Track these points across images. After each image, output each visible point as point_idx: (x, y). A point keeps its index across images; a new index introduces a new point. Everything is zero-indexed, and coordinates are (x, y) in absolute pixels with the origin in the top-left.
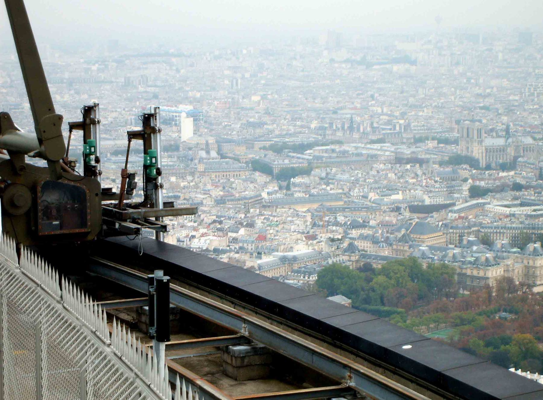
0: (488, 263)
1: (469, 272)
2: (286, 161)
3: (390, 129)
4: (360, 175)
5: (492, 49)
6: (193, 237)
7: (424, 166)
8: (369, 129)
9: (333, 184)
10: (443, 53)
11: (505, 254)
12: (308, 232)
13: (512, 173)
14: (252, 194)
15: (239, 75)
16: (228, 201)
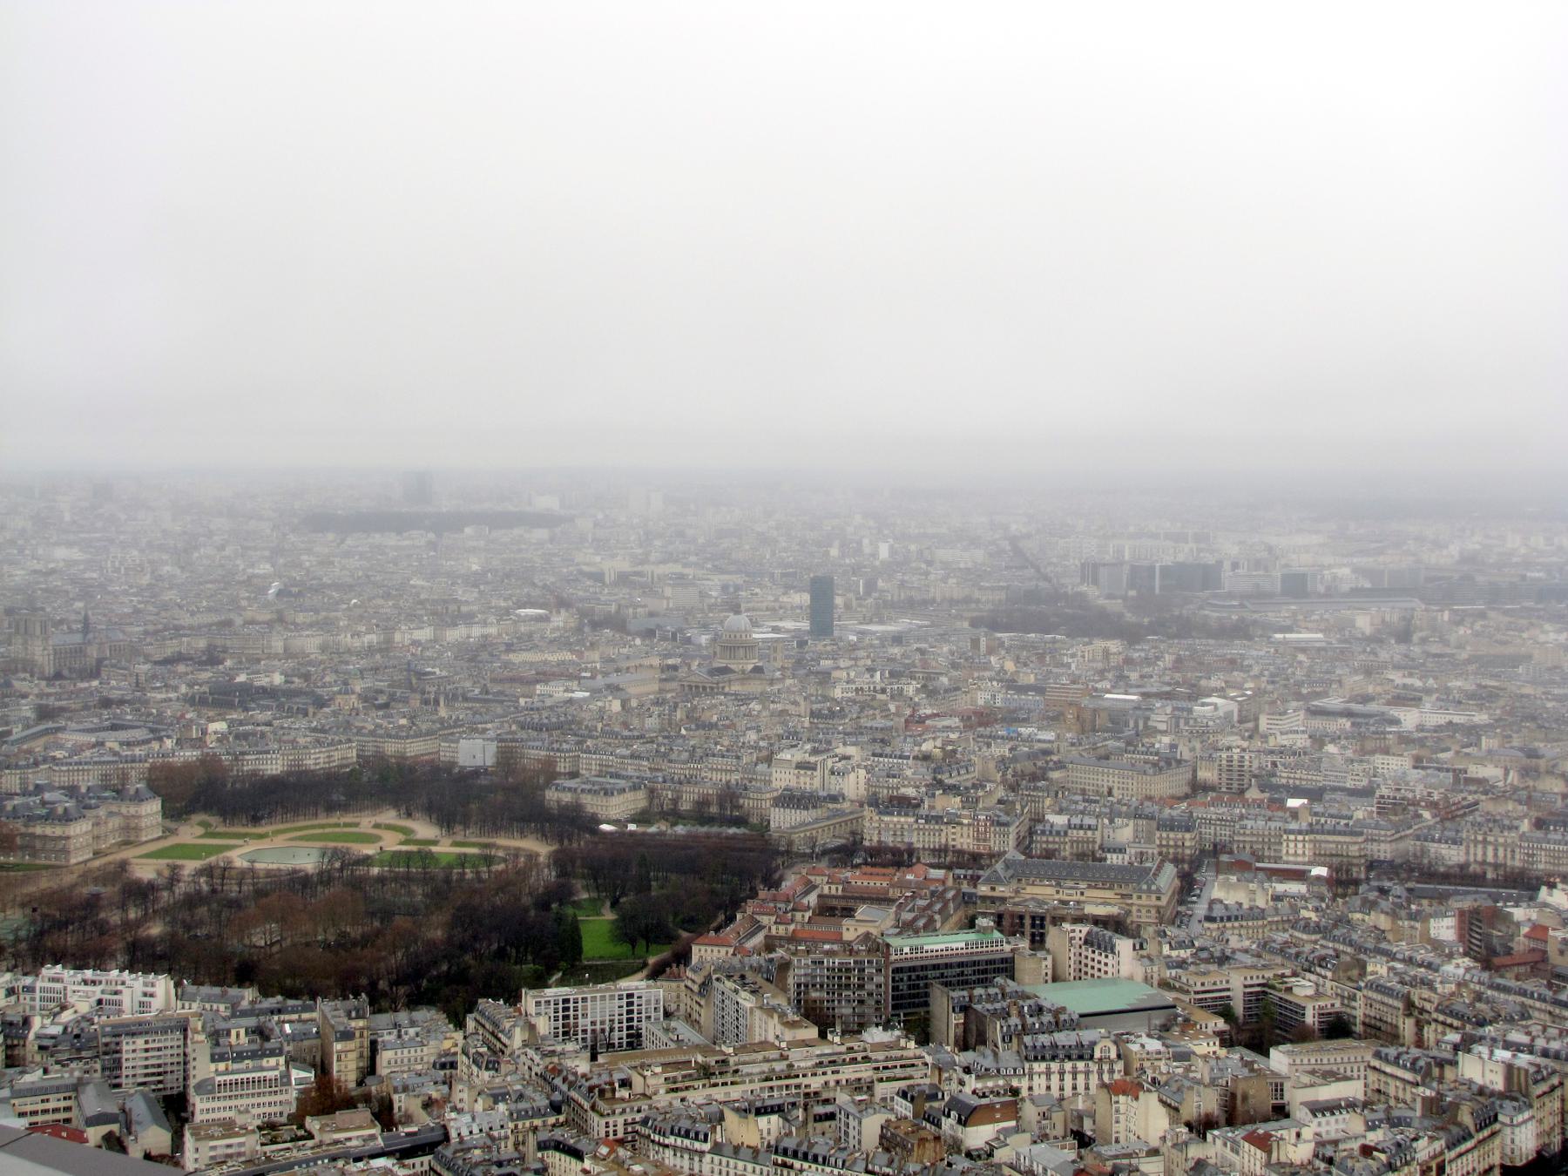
0: (67, 818)
13: (95, 683)
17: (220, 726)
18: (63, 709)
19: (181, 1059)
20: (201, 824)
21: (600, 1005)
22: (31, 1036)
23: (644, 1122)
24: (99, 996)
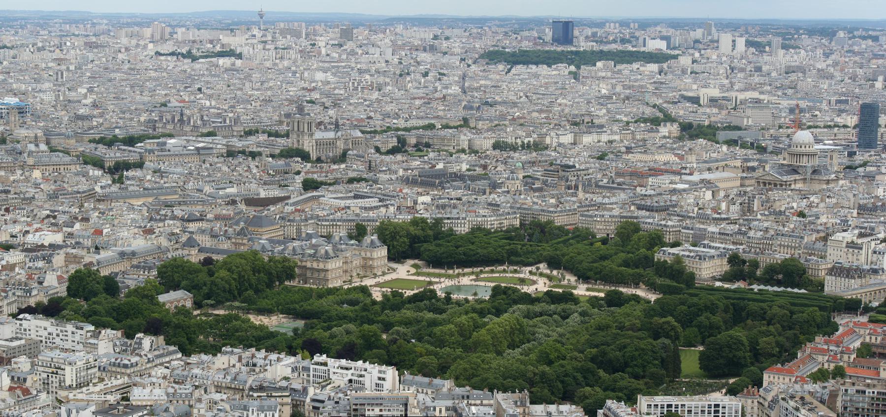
0: (327, 256)
1: (309, 265)
2: (118, 155)
4: (193, 169)
5: (314, 45)
6: (27, 232)
7: (257, 159)
8: (199, 122)
9: (167, 177)
10: (267, 47)
11: (343, 246)
12: (145, 227)
13: (343, 166)
14: (85, 188)
15: (63, 67)
20: (415, 266)
22: (308, 400)
24: (350, 377)
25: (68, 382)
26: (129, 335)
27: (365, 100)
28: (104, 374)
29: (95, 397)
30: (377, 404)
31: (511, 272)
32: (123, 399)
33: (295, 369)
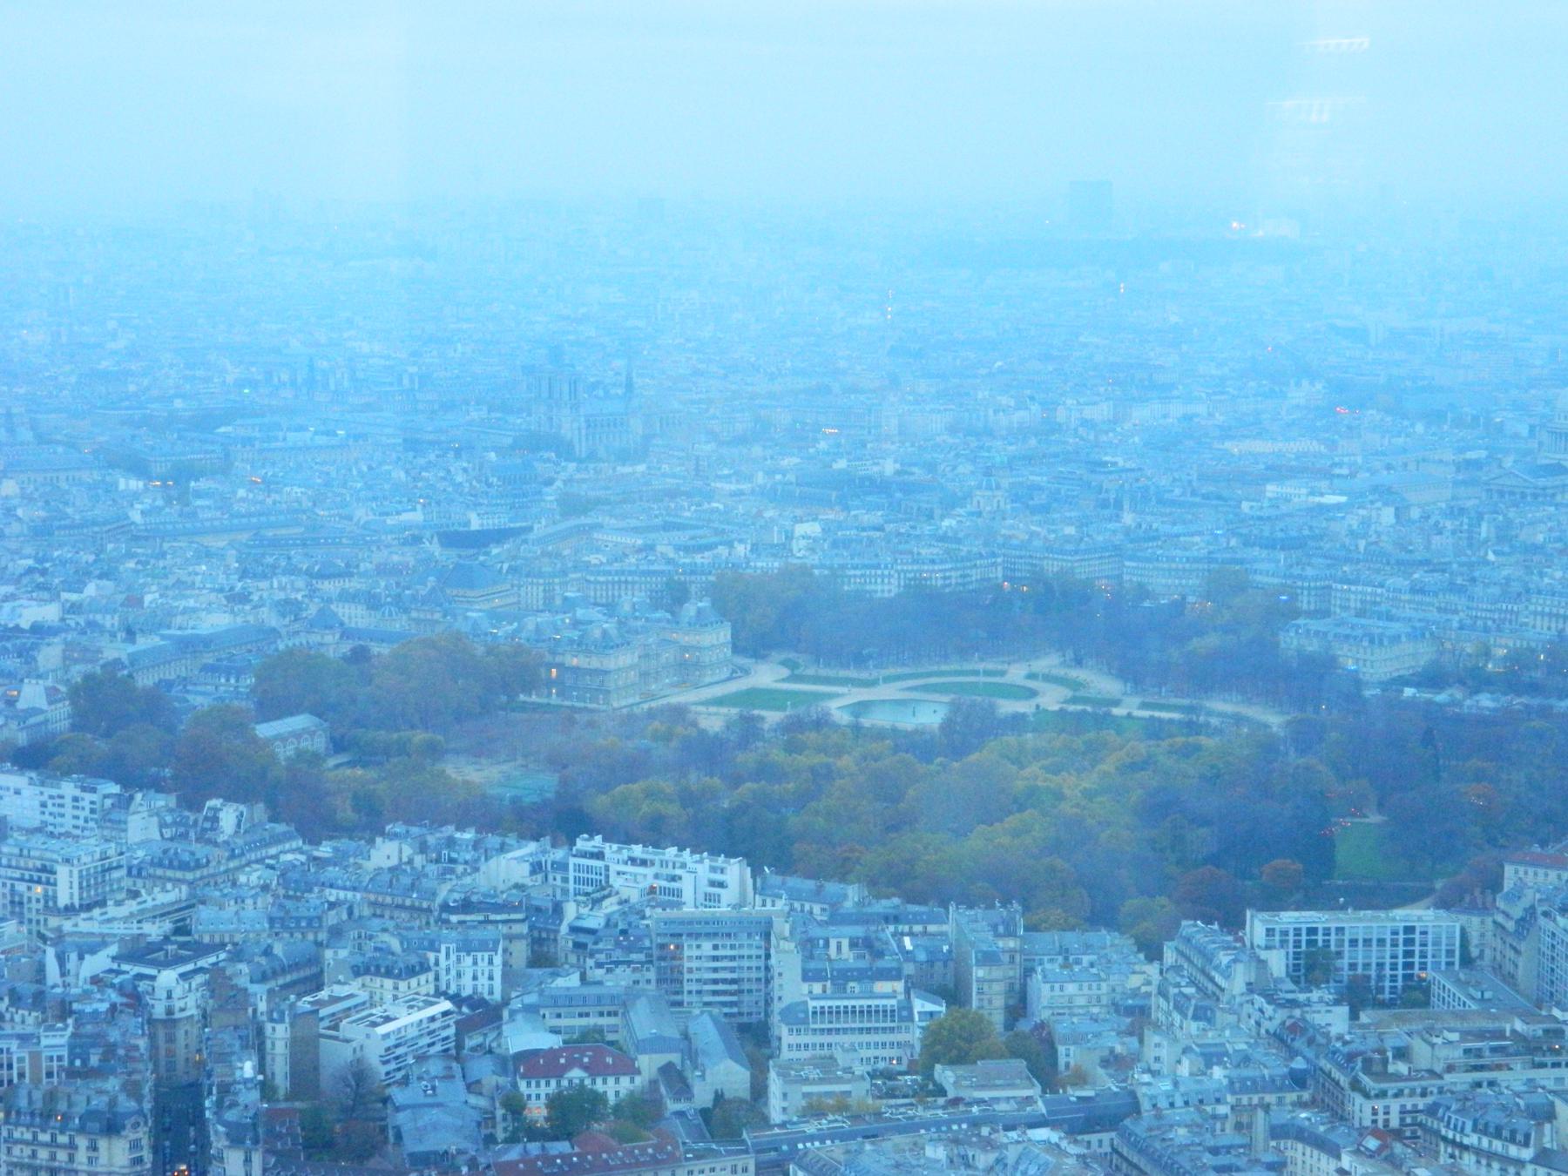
0: (607, 645)
3: (391, 384)
8: (346, 384)
12: (232, 589)
13: (641, 468)
16: (59, 528)
17: (813, 528)
18: (599, 501)
19: (762, 975)
20: (784, 663)
21: (1364, 931)
22: (564, 929)
23: (1432, 1110)
24: (650, 881)
25: (63, 901)
26: (192, 801)
27: (688, 340)
28: (140, 882)
29: (118, 929)
30: (708, 935)
31: (988, 673)
32: (178, 931)
33: (537, 868)
